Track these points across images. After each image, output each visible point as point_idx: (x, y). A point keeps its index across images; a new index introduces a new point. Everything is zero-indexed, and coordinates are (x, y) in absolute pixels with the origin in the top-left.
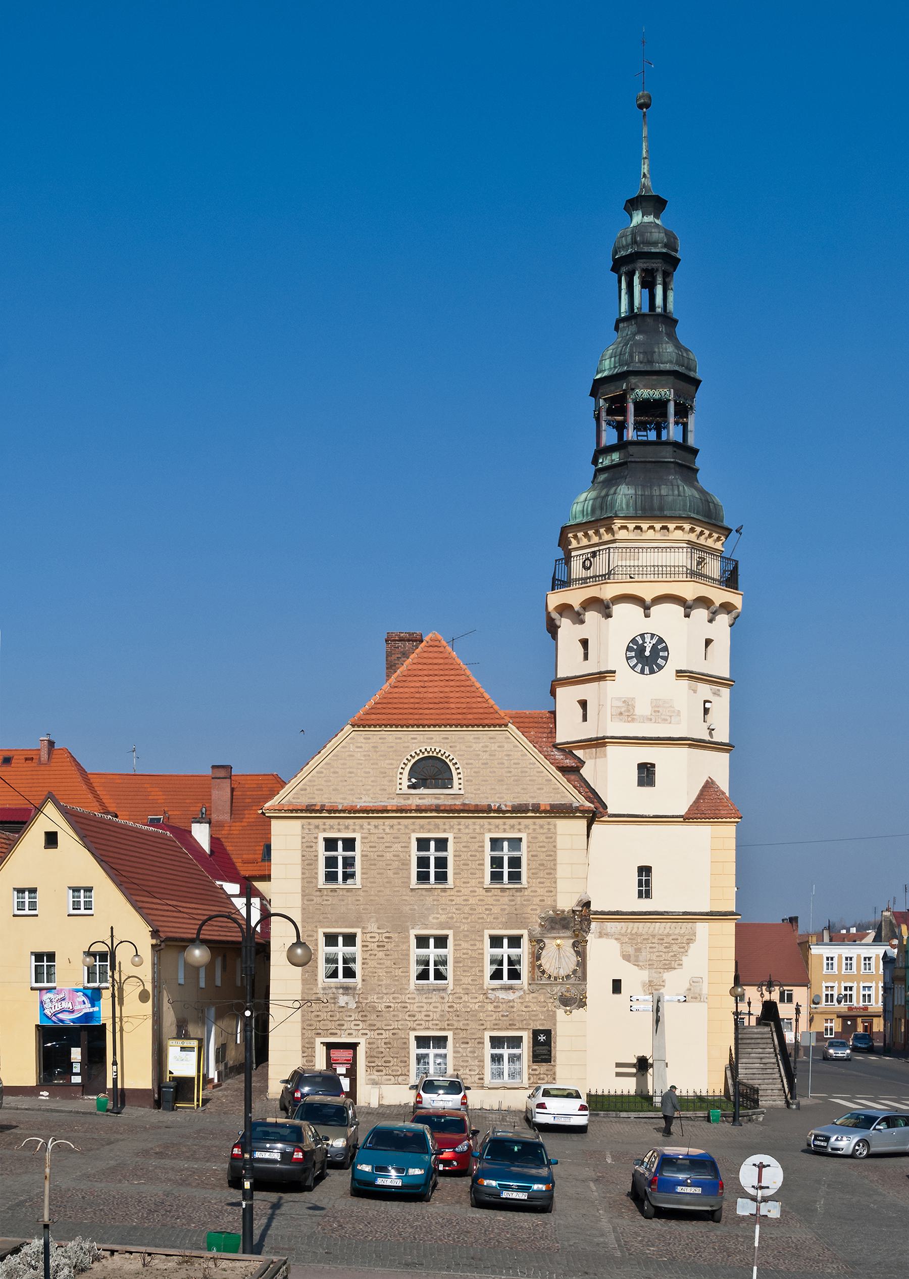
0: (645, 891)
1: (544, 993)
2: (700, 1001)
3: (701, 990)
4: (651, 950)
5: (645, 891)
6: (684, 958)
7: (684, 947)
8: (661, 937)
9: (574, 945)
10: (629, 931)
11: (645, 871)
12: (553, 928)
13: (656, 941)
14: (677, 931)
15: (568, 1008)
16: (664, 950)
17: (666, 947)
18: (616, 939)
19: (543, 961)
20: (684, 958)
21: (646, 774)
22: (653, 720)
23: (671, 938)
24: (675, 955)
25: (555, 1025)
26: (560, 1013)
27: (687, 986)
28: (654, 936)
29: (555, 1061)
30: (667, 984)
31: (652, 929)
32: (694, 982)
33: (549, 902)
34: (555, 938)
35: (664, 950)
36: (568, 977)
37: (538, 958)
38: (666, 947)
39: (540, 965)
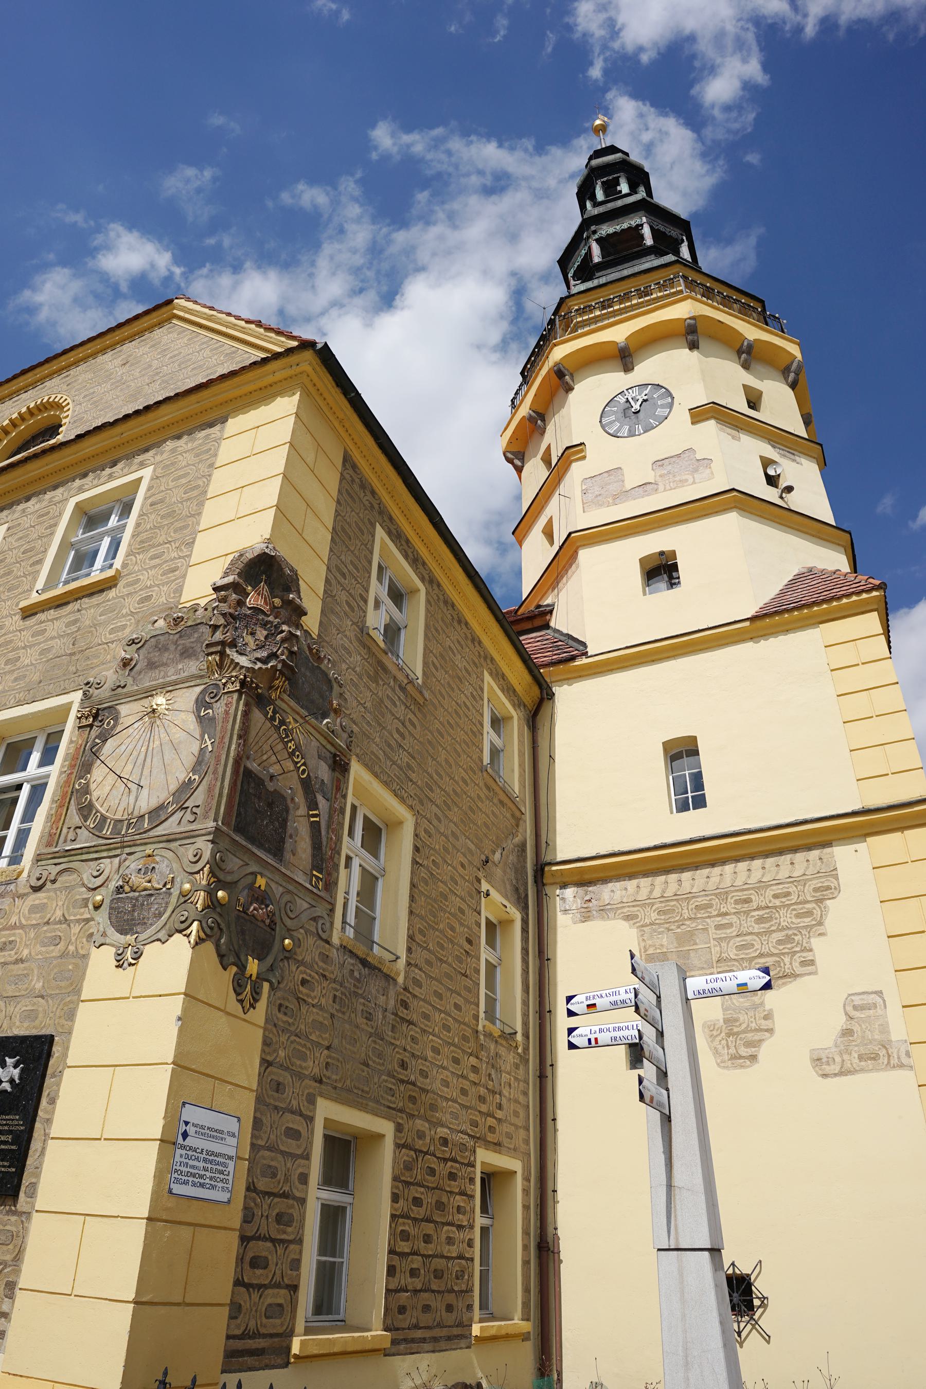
0: (691, 796)
1: (69, 889)
2: (890, 1066)
3: (884, 1029)
4: (721, 933)
5: (691, 796)
6: (815, 942)
7: (809, 913)
8: (743, 895)
9: (201, 703)
10: (657, 893)
11: (682, 751)
12: (152, 665)
13: (730, 907)
14: (783, 874)
15: (130, 938)
16: (757, 928)
17: (761, 920)
18: (628, 918)
19: (98, 773)
20: (815, 942)
21: (661, 570)
22: (661, 487)
23: (770, 893)
24: (789, 939)
25: (71, 1015)
26: (102, 960)
27: (840, 1021)
28: (723, 895)
29: (32, 1195)
30: (779, 1023)
31: (715, 879)
32: (862, 1007)
33: (161, 598)
34: (149, 693)
35: (757, 928)
36: (158, 814)
37: (87, 768)
38: (761, 920)
39: (86, 790)
